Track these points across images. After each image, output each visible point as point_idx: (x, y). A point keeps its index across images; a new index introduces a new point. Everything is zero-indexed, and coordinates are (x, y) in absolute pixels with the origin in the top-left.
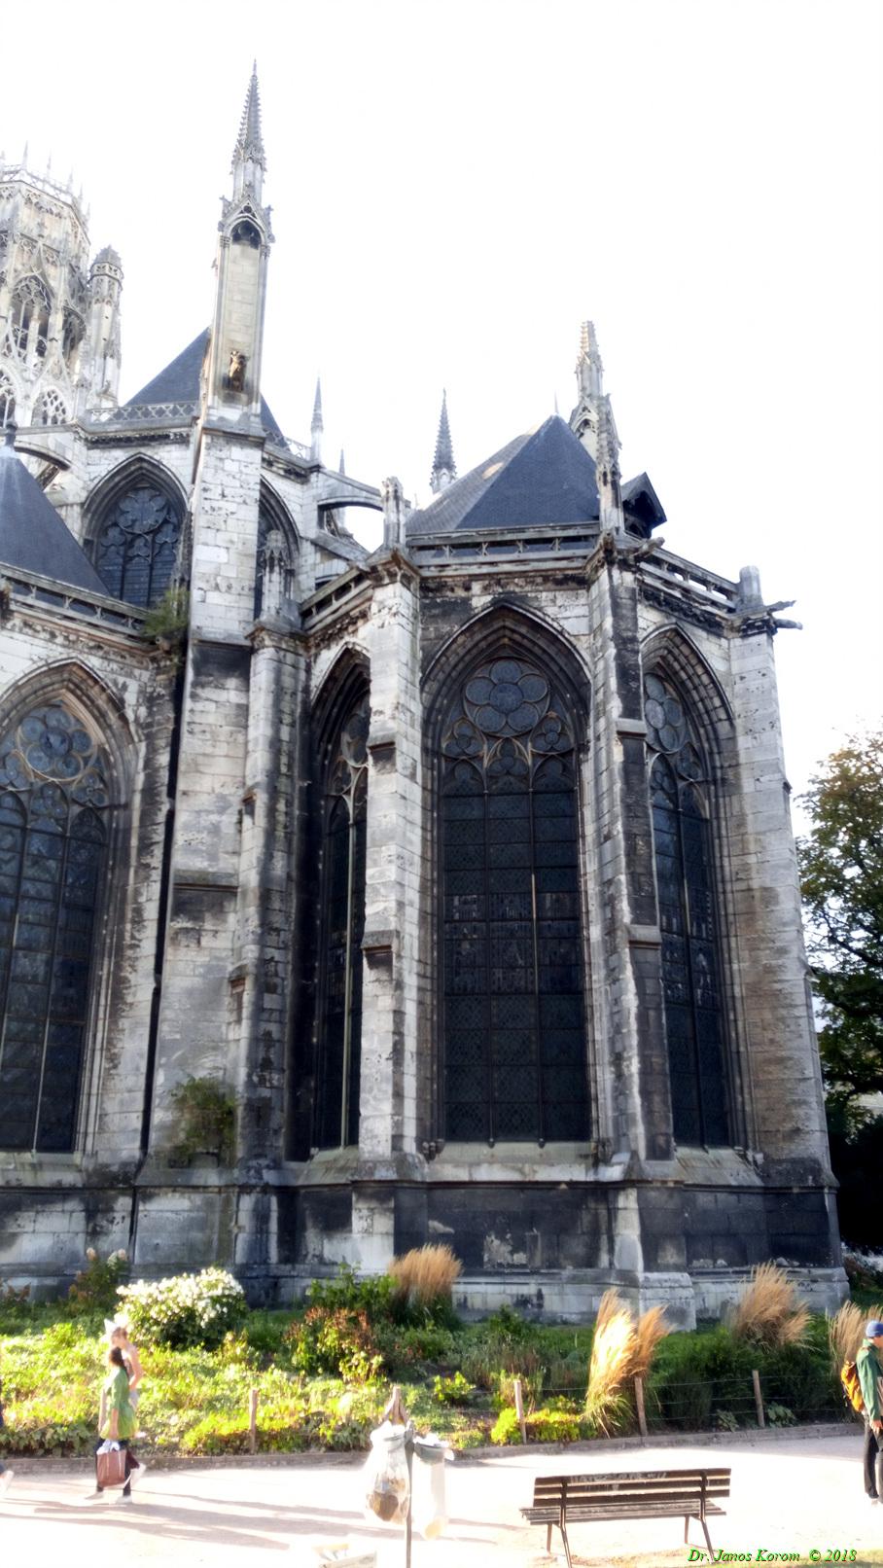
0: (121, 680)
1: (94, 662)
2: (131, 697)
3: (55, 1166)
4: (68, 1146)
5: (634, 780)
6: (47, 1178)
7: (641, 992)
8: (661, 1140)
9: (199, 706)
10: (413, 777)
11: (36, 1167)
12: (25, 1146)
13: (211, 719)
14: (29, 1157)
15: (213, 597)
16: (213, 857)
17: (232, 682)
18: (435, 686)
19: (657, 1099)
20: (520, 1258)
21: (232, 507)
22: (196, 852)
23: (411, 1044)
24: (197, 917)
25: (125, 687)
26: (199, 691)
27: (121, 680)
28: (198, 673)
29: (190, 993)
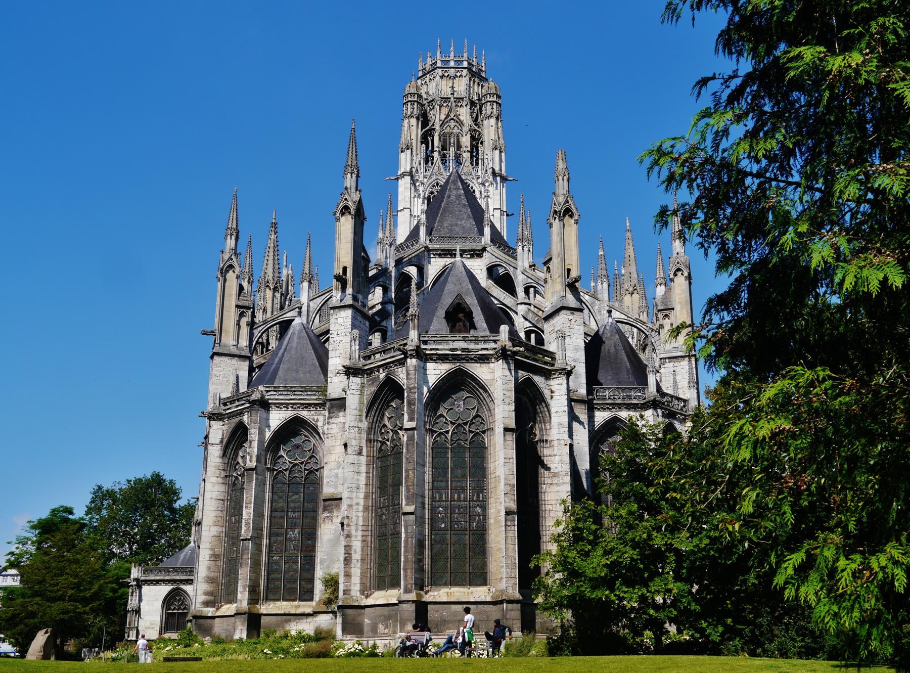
0: (316, 418)
1: (304, 414)
2: (320, 424)
3: (304, 606)
4: (311, 599)
5: (410, 447)
6: (299, 611)
7: (406, 532)
8: (409, 586)
9: (330, 427)
10: (360, 453)
11: (297, 607)
12: (295, 600)
13: (334, 431)
14: (296, 603)
15: (335, 379)
16: (336, 487)
17: (341, 414)
18: (373, 413)
19: (409, 571)
20: (386, 631)
21: (341, 338)
22: (330, 486)
23: (356, 556)
24: (331, 511)
25: (318, 420)
26: (330, 420)
27: (316, 418)
28: (329, 413)
29: (329, 541)
